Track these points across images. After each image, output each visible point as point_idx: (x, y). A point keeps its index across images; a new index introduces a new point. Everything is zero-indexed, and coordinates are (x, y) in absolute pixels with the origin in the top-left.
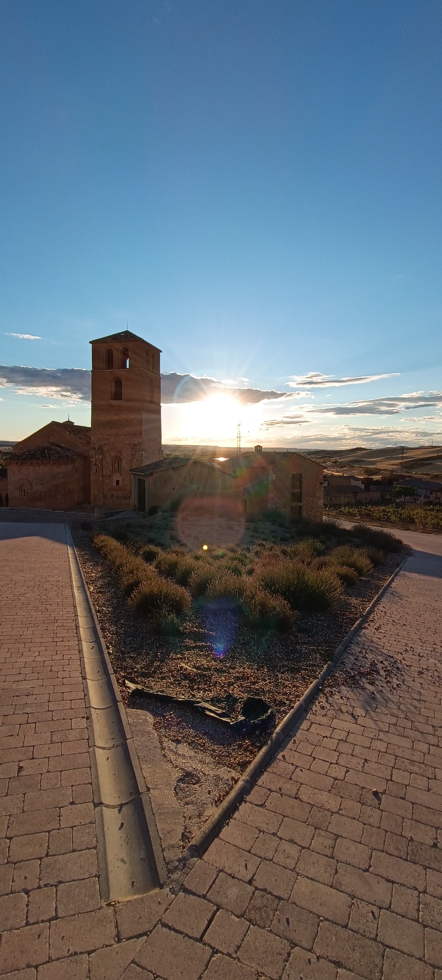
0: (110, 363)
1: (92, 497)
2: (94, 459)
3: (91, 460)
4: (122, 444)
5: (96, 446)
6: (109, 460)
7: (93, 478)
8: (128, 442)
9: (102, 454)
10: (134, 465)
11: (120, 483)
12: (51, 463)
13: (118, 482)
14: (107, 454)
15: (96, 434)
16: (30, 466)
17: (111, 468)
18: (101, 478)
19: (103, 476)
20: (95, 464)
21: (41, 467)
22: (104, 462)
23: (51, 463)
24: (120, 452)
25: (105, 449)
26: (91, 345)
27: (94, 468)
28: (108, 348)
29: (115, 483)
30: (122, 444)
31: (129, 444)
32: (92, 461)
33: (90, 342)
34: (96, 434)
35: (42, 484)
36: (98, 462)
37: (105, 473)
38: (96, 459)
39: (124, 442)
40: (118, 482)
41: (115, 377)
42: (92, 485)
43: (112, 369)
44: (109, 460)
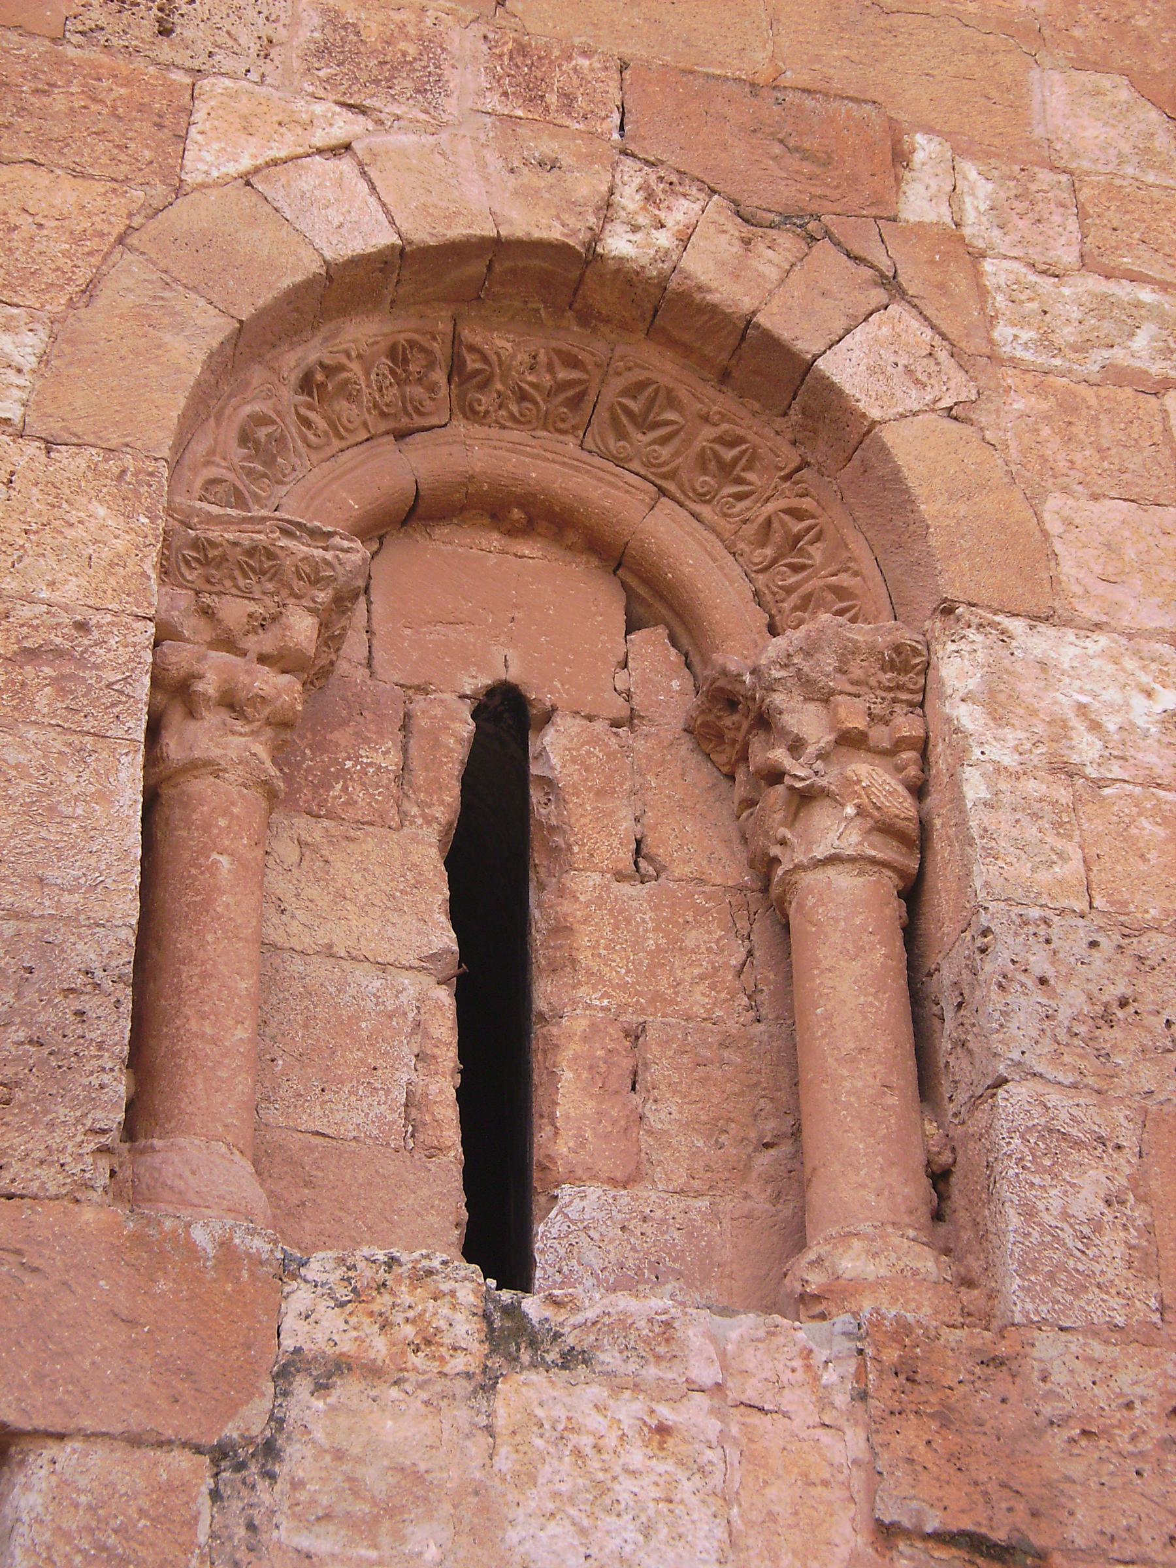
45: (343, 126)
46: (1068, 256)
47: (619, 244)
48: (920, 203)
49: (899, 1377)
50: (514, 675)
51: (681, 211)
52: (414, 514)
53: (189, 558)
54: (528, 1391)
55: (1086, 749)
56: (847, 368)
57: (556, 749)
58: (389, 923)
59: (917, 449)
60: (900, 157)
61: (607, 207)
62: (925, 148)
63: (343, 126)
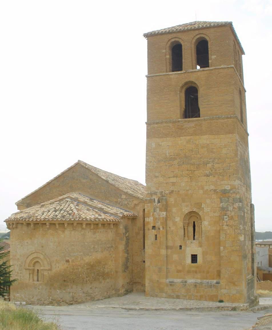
0: (177, 64)
1: (147, 285)
2: (152, 218)
3: (147, 220)
4: (201, 192)
5: (154, 197)
6: (178, 219)
7: (149, 250)
8: (212, 187)
9: (166, 208)
10: (225, 227)
11: (199, 259)
12: (84, 226)
13: (194, 258)
14: (174, 210)
15: (156, 177)
16: (49, 229)
17: (181, 232)
18: (163, 252)
19: (167, 248)
20: (154, 227)
21: (67, 232)
22: (170, 223)
23: (84, 226)
24: (199, 205)
25: (172, 200)
26: (145, 41)
27: (150, 235)
28: (173, 40)
29: (189, 260)
30: (201, 192)
31: (215, 190)
32: (148, 222)
33: (146, 36)
34: (156, 177)
35: (68, 261)
36: (158, 224)
37: (170, 244)
38: (155, 219)
39: (206, 188)
40: (194, 258)
41: (186, 83)
42: (147, 264)
43: (181, 70)
44: (178, 219)
45: (186, 208)
46: (207, 207)
47: (194, 211)
48: (202, 206)
49: (199, 243)
50: (194, 221)
51: (195, 209)
52: (191, 217)
53: (184, 223)
54: (191, 244)
55: (205, 225)
56: (200, 214)
57: (195, 223)
58: (191, 229)
59: (202, 217)
60: (202, 205)
61: (193, 209)
62: (203, 204)
63: (186, 208)
